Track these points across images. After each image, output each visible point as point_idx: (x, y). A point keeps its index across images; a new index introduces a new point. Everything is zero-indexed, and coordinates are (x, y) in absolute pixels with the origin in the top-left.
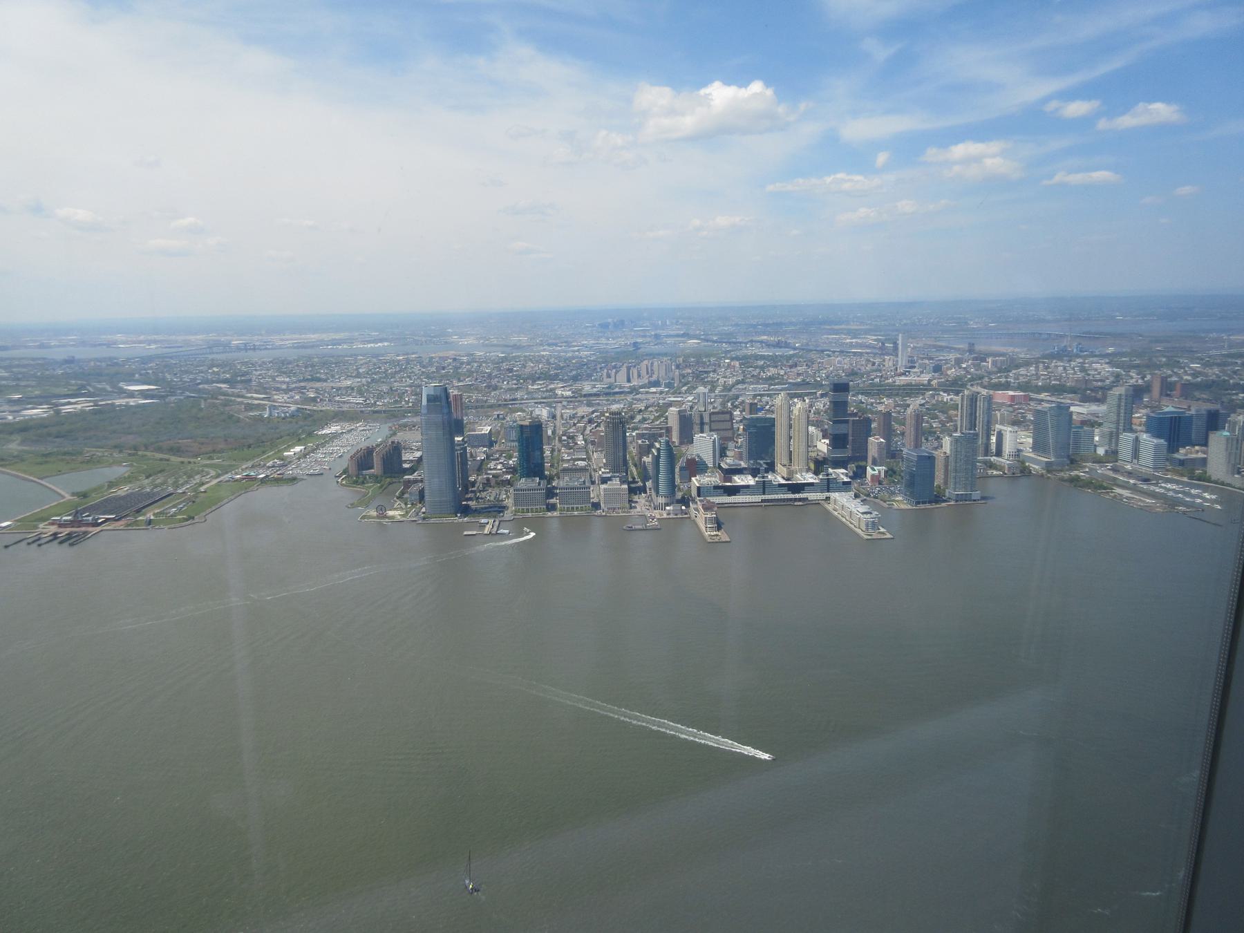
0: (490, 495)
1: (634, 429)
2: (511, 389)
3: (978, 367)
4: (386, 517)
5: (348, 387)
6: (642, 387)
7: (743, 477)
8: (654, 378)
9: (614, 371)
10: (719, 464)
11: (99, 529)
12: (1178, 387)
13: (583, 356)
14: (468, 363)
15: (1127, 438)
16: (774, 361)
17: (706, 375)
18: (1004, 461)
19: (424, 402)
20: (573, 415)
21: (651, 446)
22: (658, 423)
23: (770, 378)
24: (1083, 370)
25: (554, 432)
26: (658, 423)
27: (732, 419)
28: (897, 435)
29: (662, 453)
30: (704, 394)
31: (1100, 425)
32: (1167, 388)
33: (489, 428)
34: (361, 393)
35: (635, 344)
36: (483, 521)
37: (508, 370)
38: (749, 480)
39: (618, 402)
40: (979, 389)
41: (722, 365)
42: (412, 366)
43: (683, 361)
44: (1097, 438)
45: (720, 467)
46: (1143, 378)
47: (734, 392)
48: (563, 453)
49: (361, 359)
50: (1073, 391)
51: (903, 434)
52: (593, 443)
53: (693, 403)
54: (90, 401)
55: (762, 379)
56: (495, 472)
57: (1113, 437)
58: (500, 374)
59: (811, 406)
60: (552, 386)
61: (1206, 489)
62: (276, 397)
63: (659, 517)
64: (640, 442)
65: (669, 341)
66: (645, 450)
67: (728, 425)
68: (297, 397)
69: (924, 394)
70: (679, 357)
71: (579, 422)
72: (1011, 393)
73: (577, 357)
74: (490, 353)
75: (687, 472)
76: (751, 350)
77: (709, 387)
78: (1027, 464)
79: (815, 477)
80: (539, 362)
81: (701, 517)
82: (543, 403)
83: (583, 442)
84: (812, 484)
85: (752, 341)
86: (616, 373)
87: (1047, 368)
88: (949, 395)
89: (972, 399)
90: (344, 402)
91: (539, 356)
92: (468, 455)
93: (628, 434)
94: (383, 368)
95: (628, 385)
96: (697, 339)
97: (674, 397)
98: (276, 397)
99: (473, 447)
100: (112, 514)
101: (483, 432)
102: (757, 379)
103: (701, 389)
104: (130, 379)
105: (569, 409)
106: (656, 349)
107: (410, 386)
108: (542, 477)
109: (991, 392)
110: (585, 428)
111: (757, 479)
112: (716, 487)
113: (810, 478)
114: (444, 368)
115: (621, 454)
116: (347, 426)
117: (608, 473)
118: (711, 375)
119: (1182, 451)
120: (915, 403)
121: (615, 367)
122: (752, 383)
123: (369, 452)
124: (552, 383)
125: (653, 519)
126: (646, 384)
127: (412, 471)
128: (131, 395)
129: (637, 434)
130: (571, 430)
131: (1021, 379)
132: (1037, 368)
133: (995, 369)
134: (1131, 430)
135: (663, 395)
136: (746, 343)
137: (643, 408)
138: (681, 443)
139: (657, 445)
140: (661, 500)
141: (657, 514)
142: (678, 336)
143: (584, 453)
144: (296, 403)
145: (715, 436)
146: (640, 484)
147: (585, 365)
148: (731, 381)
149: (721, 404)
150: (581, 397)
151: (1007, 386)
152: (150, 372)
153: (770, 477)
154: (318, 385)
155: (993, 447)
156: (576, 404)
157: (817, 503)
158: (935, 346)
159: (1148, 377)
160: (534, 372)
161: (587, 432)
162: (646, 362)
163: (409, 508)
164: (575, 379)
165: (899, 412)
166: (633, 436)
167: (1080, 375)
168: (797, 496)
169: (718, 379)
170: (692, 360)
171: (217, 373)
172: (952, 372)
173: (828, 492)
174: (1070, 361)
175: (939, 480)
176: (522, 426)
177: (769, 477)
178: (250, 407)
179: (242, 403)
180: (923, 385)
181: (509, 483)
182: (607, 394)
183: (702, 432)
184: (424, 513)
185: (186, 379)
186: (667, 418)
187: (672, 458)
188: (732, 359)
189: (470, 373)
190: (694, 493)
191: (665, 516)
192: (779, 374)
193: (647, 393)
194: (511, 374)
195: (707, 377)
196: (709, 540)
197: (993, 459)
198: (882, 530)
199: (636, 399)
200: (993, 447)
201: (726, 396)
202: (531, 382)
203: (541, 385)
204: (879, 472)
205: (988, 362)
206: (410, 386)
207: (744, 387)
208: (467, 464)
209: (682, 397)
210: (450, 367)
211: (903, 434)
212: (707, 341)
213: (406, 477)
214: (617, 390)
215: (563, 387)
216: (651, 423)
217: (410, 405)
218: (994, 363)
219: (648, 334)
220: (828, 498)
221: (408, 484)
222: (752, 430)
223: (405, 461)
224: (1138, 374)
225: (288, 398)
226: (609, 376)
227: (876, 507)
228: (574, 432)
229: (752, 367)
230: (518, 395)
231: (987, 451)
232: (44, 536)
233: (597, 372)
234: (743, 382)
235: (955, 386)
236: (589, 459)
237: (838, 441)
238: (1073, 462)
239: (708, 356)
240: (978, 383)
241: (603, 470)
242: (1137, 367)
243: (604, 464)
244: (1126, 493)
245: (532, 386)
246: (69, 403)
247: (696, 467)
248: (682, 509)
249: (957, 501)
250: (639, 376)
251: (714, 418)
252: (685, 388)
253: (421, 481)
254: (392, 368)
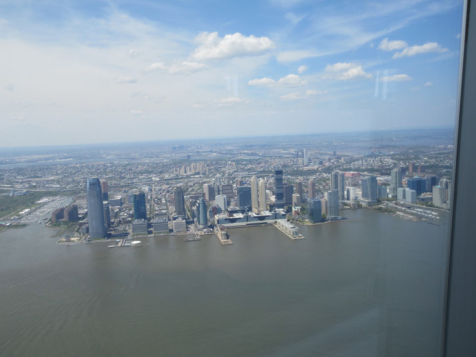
0: (121, 228)
1: (188, 194)
2: (131, 178)
3: (338, 162)
4: (70, 241)
5: (52, 180)
6: (192, 175)
7: (238, 214)
8: (197, 171)
9: (179, 168)
10: (227, 209)
12: (419, 167)
13: (165, 162)
14: (111, 167)
15: (400, 190)
16: (251, 162)
17: (220, 169)
18: (351, 202)
19: (88, 186)
20: (160, 189)
21: (196, 202)
22: (199, 191)
23: (249, 169)
24: (381, 161)
25: (151, 197)
26: (199, 191)
27: (232, 188)
28: (305, 193)
29: (201, 205)
30: (219, 177)
31: (389, 185)
32: (415, 168)
33: (120, 197)
34: (58, 183)
35: (188, 156)
36: (118, 240)
37: (130, 169)
38: (241, 216)
39: (181, 182)
40: (339, 171)
41: (227, 164)
42: (84, 169)
43: (210, 163)
44: (388, 191)
45: (227, 210)
46: (405, 164)
47: (233, 176)
48: (155, 207)
49: (59, 167)
50: (377, 171)
51: (307, 192)
52: (169, 201)
53: (215, 181)
55: (245, 170)
56: (123, 217)
57: (395, 190)
58: (126, 171)
59: (267, 181)
60: (150, 176)
61: (433, 211)
62: (16, 186)
63: (200, 234)
64: (191, 200)
65: (204, 154)
66: (193, 204)
67: (230, 191)
68: (27, 186)
69: (315, 174)
70: (208, 161)
71: (163, 192)
72: (352, 172)
73: (162, 162)
74: (121, 162)
75: (213, 213)
76: (240, 157)
77: (222, 174)
78: (360, 203)
79: (270, 213)
80: (144, 165)
81: (219, 234)
82: (146, 184)
83: (165, 201)
84: (268, 216)
85: (240, 153)
86: (179, 170)
87: (366, 161)
88: (326, 174)
89: (335, 176)
90: (50, 187)
91: (144, 163)
92: (110, 210)
93: (185, 197)
94: (69, 170)
95: (185, 174)
96: (216, 153)
97: (206, 179)
98: (16, 186)
99: (113, 206)
101: (117, 199)
102: (243, 170)
103: (218, 175)
105: (158, 186)
106: (198, 158)
107: (83, 179)
108: (145, 218)
109: (344, 172)
110: (166, 194)
111: (244, 215)
112: (226, 219)
113: (267, 213)
114: (99, 169)
115: (182, 206)
116: (51, 198)
117: (176, 215)
118: (223, 169)
119: (422, 195)
120: (312, 178)
121: (179, 167)
122: (241, 172)
123: (62, 210)
124: (150, 175)
125: (198, 236)
126: (193, 174)
127: (83, 218)
129: (189, 196)
130: (159, 196)
131: (356, 166)
132: (362, 161)
133: (345, 163)
134: (402, 187)
135: (201, 179)
136: (238, 154)
137: (192, 185)
138: (210, 200)
139: (198, 201)
140: (201, 227)
141: (199, 233)
142: (207, 152)
143: (165, 206)
144: (26, 188)
145: (225, 196)
146: (192, 219)
147: (165, 166)
148: (232, 171)
149: (227, 182)
150: (164, 180)
151: (350, 170)
153: (250, 213)
154: (37, 179)
155: (346, 196)
156: (162, 184)
157: (271, 224)
158: (319, 153)
159: (407, 164)
160: (141, 170)
161: (167, 197)
162: (193, 164)
163: (82, 236)
164: (161, 172)
165: (305, 182)
166: (188, 198)
167: (380, 164)
168: (262, 222)
169: (226, 170)
170: (214, 162)
172: (327, 164)
173: (276, 219)
174: (375, 158)
175: (323, 212)
176: (135, 195)
177: (249, 213)
180: (315, 170)
181: (130, 222)
182: (176, 179)
183: (219, 194)
184: (89, 238)
186: (203, 189)
187: (205, 207)
188: (232, 161)
189: (112, 171)
190: (216, 222)
191: (203, 234)
192: (253, 167)
193: (194, 178)
194: (131, 171)
195: (221, 170)
196: (223, 244)
197: (346, 201)
198: (300, 235)
199: (189, 181)
200: (346, 196)
201: (229, 178)
202: (140, 174)
203: (145, 176)
204: (298, 209)
205: (342, 159)
206: (83, 179)
207: (237, 174)
208: (110, 214)
209: (210, 179)
210: (102, 169)
211: (307, 192)
212: (221, 153)
213: (80, 221)
214: (180, 177)
215: (155, 176)
216: (196, 191)
217: (83, 187)
218: (344, 160)
219: (194, 151)
220: (276, 222)
221: (81, 224)
222: (242, 193)
223: (80, 214)
224: (403, 163)
225: (23, 186)
226: (176, 171)
227: (297, 225)
228: (160, 197)
229: (240, 165)
230: (134, 181)
231: (343, 198)
233: (171, 169)
234: (237, 171)
235: (328, 170)
236: (167, 209)
237: (279, 196)
238: (379, 202)
239: (221, 160)
240: (338, 169)
241: (174, 214)
242: (402, 160)
243: (175, 211)
244: (401, 214)
245: (141, 176)
247: (216, 210)
248: (211, 230)
249: (331, 221)
250: (190, 170)
251: (224, 188)
252: (211, 175)
253: (87, 223)
254: (74, 170)
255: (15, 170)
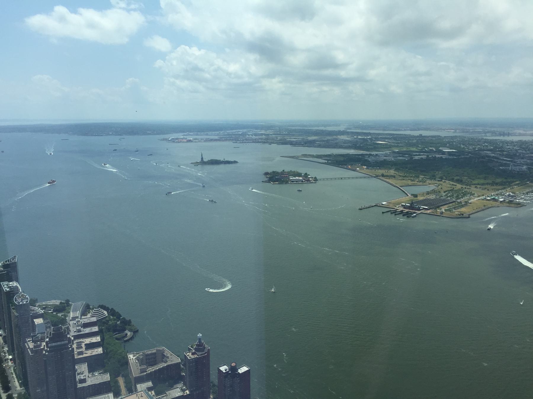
11: (419, 212)
54: (426, 155)
62: (516, 160)
100: (427, 206)
104: (445, 145)
128: (444, 153)
152: (454, 143)
171: (487, 146)
178: (502, 165)
179: (497, 162)
185: (471, 148)
225: (523, 162)
232: (398, 211)
246: (417, 155)
255: (517, 143)
